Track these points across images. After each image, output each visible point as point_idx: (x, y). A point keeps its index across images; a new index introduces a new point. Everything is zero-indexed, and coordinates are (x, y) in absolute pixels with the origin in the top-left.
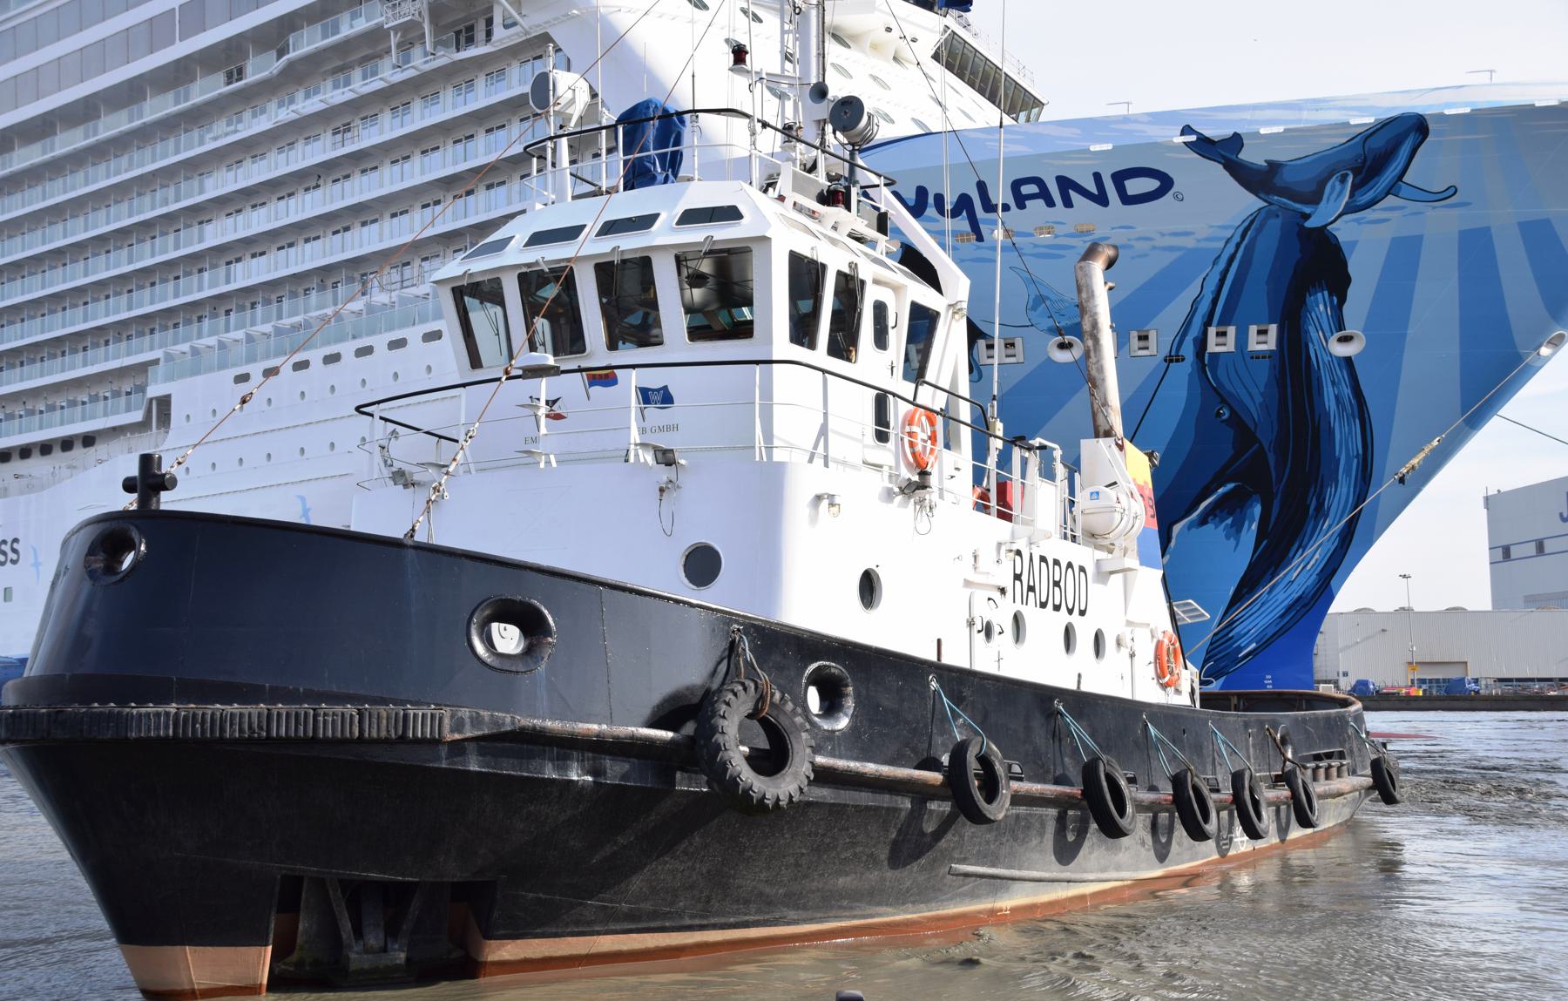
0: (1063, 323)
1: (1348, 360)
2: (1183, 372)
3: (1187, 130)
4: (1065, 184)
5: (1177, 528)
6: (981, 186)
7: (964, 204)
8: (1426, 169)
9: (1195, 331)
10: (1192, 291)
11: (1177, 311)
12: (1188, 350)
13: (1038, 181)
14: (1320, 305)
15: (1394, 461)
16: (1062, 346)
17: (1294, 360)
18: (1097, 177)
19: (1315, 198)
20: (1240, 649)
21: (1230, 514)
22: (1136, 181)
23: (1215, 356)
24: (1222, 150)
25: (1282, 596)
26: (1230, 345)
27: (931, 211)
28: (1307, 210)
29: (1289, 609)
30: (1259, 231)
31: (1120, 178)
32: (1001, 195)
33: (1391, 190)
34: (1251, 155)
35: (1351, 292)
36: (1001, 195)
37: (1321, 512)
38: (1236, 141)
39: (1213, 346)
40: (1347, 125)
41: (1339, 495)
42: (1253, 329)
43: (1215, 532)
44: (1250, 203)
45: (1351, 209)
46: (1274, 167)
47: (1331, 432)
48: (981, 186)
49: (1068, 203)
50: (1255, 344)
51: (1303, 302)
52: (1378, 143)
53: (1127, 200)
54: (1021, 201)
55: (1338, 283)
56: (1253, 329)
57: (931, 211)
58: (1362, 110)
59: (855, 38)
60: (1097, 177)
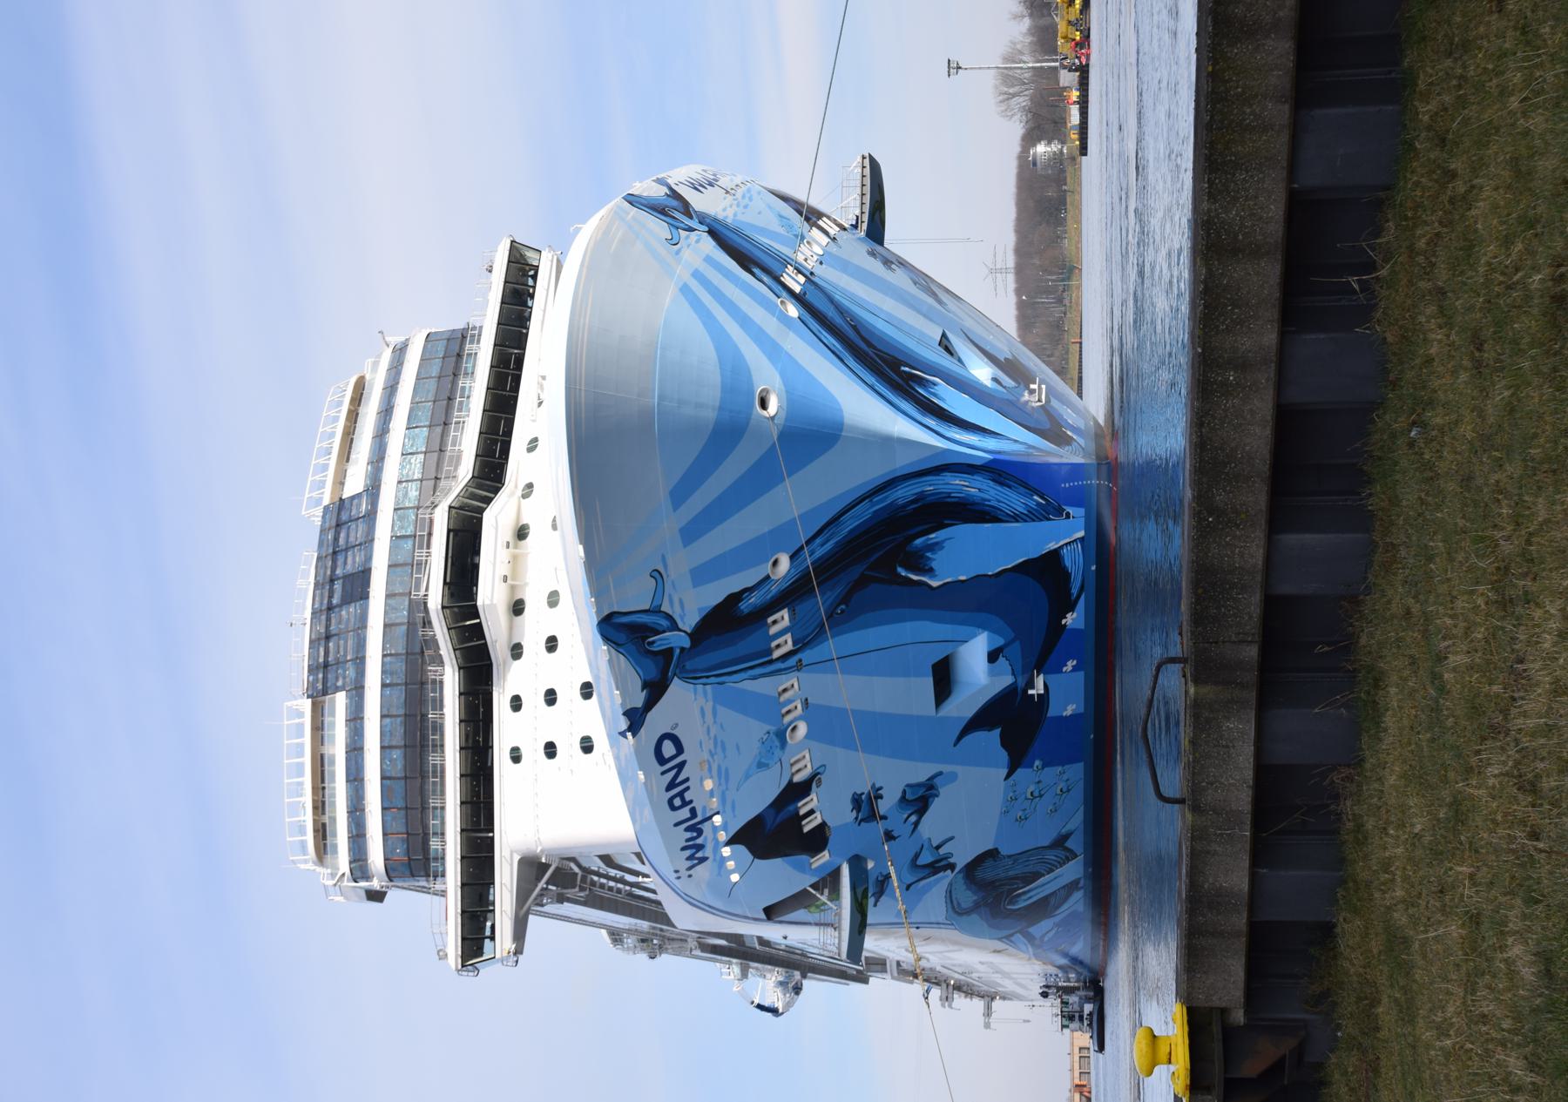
0: (777, 743)
1: (792, 557)
2: (807, 656)
3: (623, 734)
4: (670, 787)
5: (935, 584)
6: (677, 825)
7: (687, 830)
8: (635, 598)
9: (780, 665)
10: (748, 685)
11: (764, 686)
12: (792, 661)
13: (670, 802)
14: (754, 600)
15: (875, 471)
16: (794, 729)
17: (793, 594)
18: (663, 773)
19: (669, 652)
20: (1038, 504)
21: (922, 557)
22: (668, 757)
23: (794, 643)
24: (635, 719)
25: (993, 492)
26: (788, 637)
27: (699, 841)
28: (677, 651)
29: (1001, 484)
30: (695, 671)
31: (661, 760)
32: (685, 813)
33: (656, 611)
34: (639, 699)
35: (736, 589)
36: (685, 813)
37: (921, 497)
38: (628, 713)
39: (789, 646)
40: (610, 661)
41: (904, 493)
42: (773, 630)
43: (938, 560)
44: (677, 688)
45: (674, 626)
46: (645, 685)
47: (850, 532)
48: (677, 825)
49: (687, 780)
50: (786, 622)
51: (750, 614)
52: (622, 637)
53: (680, 749)
54: (685, 803)
55: (735, 598)
56: (773, 630)
57: (699, 841)
58: (596, 650)
59: (513, 588)
60: (663, 773)
